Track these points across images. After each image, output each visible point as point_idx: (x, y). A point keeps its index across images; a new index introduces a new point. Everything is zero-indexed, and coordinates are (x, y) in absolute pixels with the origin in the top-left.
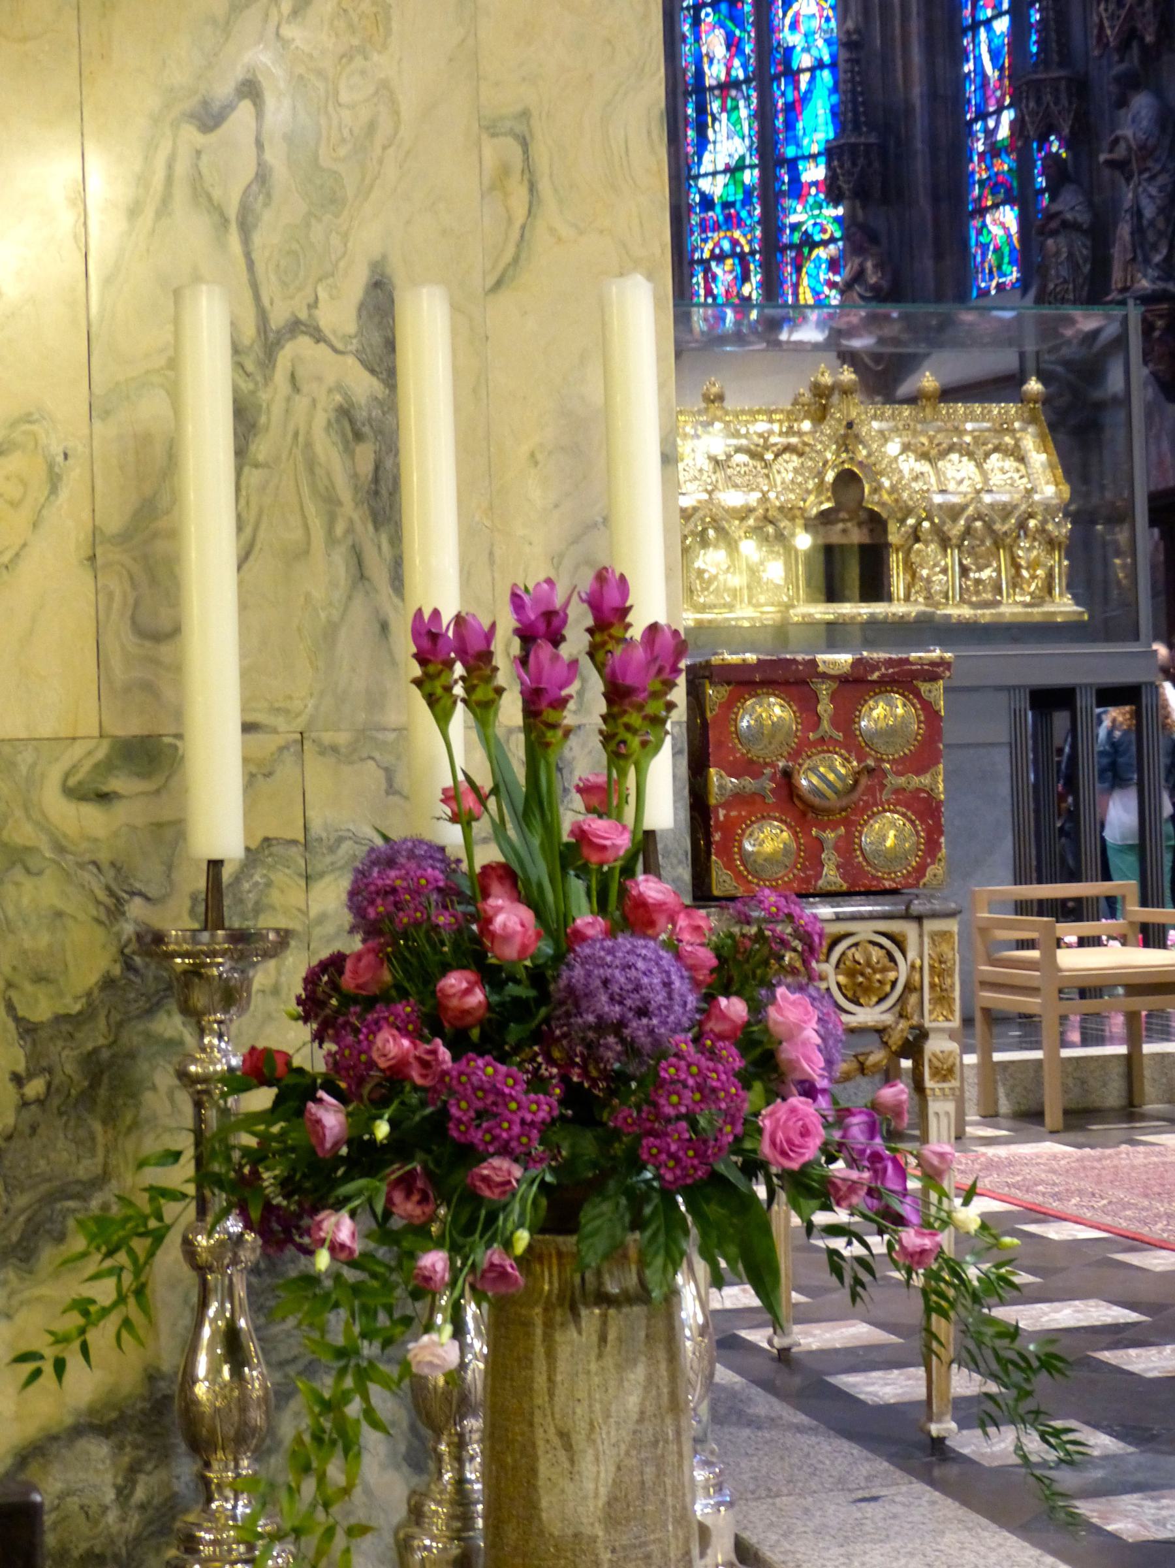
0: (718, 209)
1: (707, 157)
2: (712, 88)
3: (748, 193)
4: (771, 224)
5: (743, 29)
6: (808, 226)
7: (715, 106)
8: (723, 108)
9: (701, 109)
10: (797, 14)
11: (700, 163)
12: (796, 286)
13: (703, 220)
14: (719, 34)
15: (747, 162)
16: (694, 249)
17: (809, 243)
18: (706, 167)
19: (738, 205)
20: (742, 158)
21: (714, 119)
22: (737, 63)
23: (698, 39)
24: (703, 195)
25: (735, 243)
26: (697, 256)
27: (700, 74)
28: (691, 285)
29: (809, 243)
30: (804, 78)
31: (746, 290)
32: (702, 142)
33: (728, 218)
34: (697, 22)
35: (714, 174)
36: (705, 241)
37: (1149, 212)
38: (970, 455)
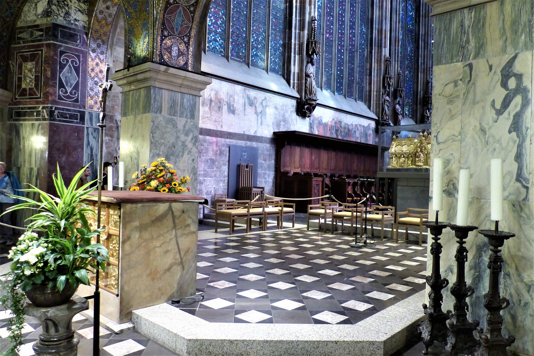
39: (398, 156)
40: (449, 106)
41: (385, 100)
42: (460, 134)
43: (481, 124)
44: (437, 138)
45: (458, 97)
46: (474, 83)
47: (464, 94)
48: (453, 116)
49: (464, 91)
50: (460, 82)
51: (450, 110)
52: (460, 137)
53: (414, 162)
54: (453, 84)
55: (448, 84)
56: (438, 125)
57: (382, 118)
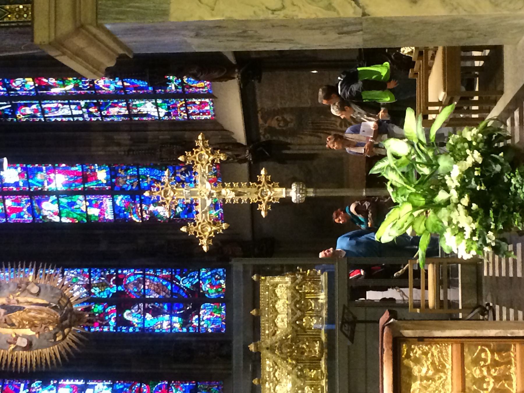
0: (170, 111)
1: (152, 114)
2: (129, 112)
3: (164, 102)
4: (176, 96)
5: (109, 102)
6: (176, 84)
7: (135, 111)
9: (136, 115)
10: (103, 86)
11: (154, 116)
12: (196, 88)
13: (174, 115)
14: (111, 110)
15: (154, 102)
16: (184, 118)
18: (156, 114)
19: (169, 105)
20: (152, 103)
21: (140, 111)
22: (120, 104)
23: (112, 116)
24: (165, 116)
26: (186, 118)
27: (124, 116)
28: (196, 120)
30: (125, 84)
31: (198, 103)
32: (147, 115)
33: (173, 108)
34: (106, 116)
35: (158, 112)
36: (181, 115)
38: (276, 301)
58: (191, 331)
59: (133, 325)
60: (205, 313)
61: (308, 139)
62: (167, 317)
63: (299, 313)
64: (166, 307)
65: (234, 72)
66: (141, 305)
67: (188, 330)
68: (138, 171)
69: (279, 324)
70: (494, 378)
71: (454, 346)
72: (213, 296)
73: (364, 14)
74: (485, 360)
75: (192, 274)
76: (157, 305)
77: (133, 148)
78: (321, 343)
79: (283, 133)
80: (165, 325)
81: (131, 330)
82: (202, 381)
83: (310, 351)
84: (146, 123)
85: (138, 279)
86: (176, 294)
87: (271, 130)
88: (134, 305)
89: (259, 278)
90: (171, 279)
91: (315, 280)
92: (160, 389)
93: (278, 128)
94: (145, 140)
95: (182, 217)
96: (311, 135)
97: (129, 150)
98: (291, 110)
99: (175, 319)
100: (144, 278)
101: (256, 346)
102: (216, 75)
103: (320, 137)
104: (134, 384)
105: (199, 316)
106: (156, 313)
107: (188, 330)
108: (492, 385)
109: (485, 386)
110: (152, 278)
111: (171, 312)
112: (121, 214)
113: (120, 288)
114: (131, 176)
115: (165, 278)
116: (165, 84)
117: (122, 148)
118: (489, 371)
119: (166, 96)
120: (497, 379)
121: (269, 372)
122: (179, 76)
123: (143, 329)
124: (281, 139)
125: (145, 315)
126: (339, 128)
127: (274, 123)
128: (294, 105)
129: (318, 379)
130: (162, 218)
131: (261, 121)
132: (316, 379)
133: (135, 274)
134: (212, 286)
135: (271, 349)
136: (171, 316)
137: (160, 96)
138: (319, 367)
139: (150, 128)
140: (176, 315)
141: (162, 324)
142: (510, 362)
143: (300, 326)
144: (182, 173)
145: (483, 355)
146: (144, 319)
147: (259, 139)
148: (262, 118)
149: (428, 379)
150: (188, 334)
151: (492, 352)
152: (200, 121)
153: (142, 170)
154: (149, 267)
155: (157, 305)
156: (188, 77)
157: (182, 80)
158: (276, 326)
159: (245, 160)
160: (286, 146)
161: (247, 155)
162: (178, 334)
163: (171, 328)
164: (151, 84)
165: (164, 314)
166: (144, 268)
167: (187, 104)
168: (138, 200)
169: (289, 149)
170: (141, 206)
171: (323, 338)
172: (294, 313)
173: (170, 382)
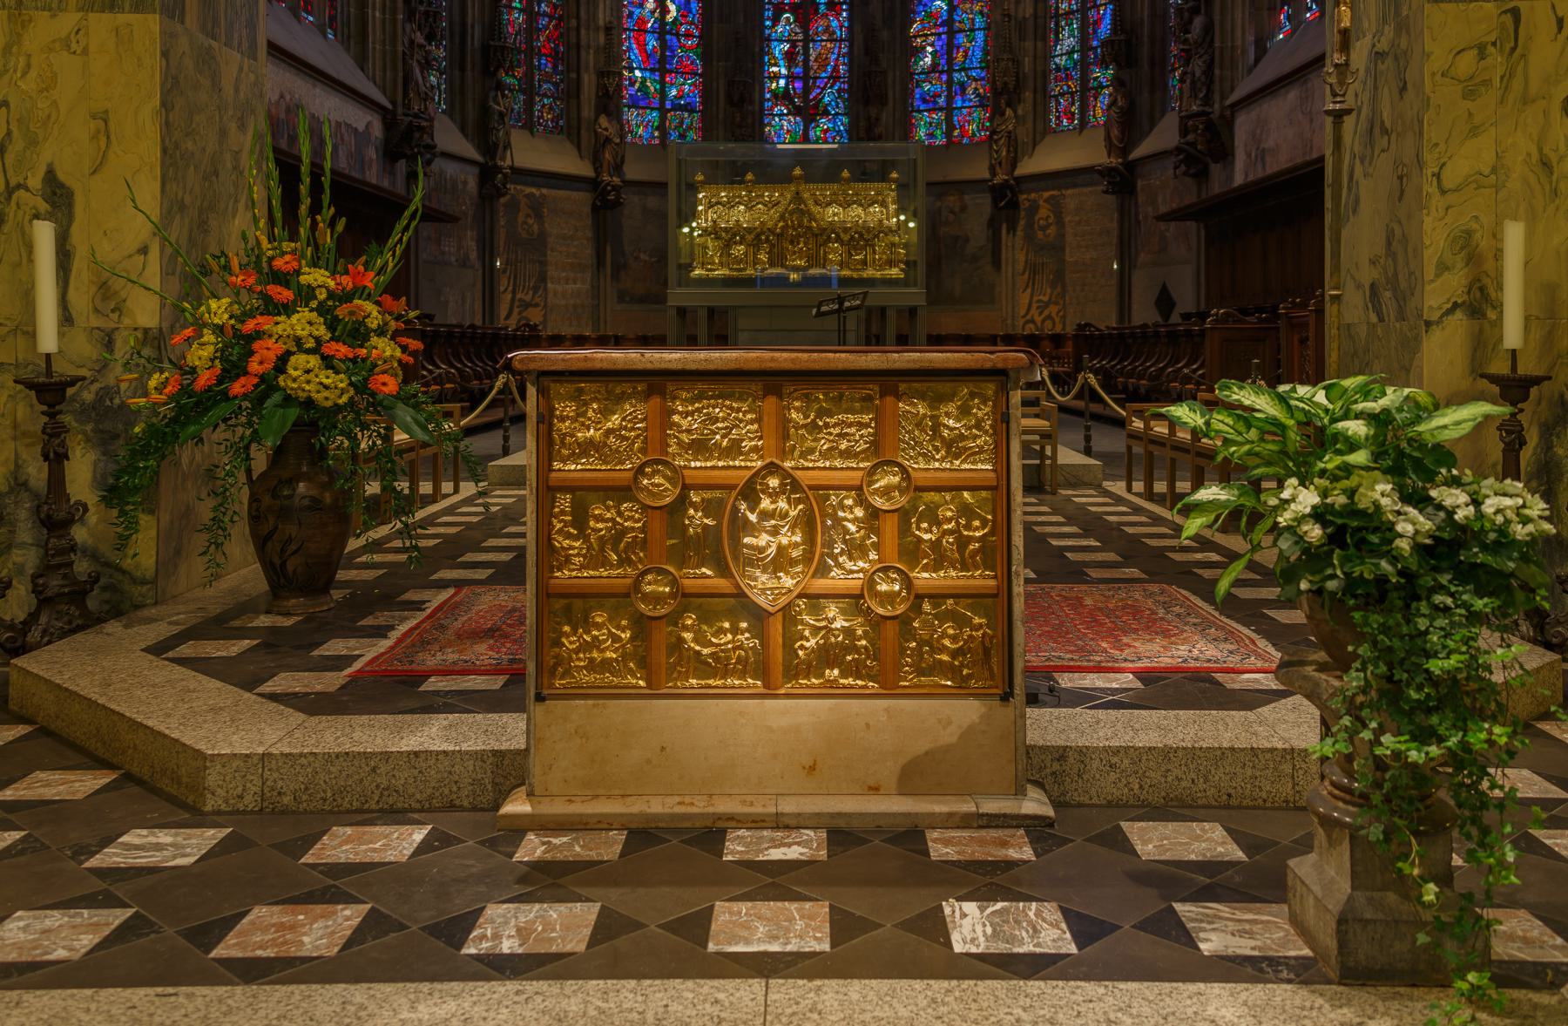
3: (1075, 64)
4: (1084, 79)
8: (1067, 24)
9: (1057, 24)
12: (1094, 107)
17: (1101, 86)
25: (1069, 87)
27: (1057, 8)
29: (1101, 86)
32: (1057, 40)
35: (1062, 55)
37: (1197, 75)
38: (861, 205)
39: (726, 237)
40: (1468, 104)
41: (412, 42)
42: (1494, 170)
43: (1540, 150)
44: (1438, 178)
45: (1487, 83)
46: (1523, 56)
47: (1502, 77)
48: (1477, 127)
49: (1500, 72)
50: (1491, 49)
51: (1470, 114)
52: (1493, 177)
53: (777, 259)
54: (1476, 51)
55: (1463, 50)
56: (1442, 147)
57: (407, 106)
58: (767, 105)
59: (774, 25)
60: (789, 122)
61: (1021, 257)
62: (784, 71)
63: (846, 238)
64: (798, 70)
65: (1118, 157)
66: (800, 37)
67: (768, 100)
68: (979, 29)
69: (830, 211)
70: (939, 540)
71: (993, 475)
72: (812, 134)
73: (1428, 324)
74: (968, 527)
75: (841, 105)
76: (800, 58)
77: (1013, 22)
78: (805, 269)
79: (1030, 225)
80: (775, 69)
81: (768, 23)
82: (702, 120)
83: (794, 253)
84: (1045, 38)
85: (834, 33)
86: (814, 82)
87: (1034, 208)
88: (801, 27)
89: (894, 181)
90: (835, 77)
91: (891, 263)
92: (692, 63)
93: (1037, 218)
94: (1022, 38)
95: (917, 91)
96: (1026, 262)
97: (1009, 16)
98: (1061, 236)
99: (782, 82)
100: (836, 40)
101: (800, 177)
102: (1115, 132)
103: (1023, 274)
104: (697, 27)
105: (787, 115)
106: (790, 57)
107: (768, 100)
108: (926, 537)
109: (925, 525)
110: (836, 51)
111: (790, 78)
112: (921, 8)
113: (822, 7)
114: (973, 20)
115: (835, 69)
116: (1103, 64)
117: (1012, 6)
118: (951, 532)
119: (1084, 66)
120: (936, 545)
121: (763, 196)
122: (1117, 82)
123: (769, 39)
124: (1022, 223)
125: (787, 41)
126: (1035, 299)
127: (1043, 212)
128: (1069, 238)
129: (755, 264)
130: (916, 63)
131: (1046, 195)
132: (756, 262)
133: (841, 27)
134: (825, 132)
135: (798, 197)
136: (787, 77)
137: (1084, 56)
138: (772, 265)
139: (1040, 44)
140: (787, 84)
141: (776, 65)
142: (964, 568)
143: (829, 239)
144: (976, 89)
145: (977, 523)
146: (781, 41)
147: (1022, 192)
148: (1052, 196)
149: (937, 427)
150: (763, 100)
151: (982, 539)
152: (1047, 111)
153: (980, 35)
154: (851, 47)
155: (800, 58)
156: (1110, 95)
157: (1107, 87)
158: (829, 204)
159: (994, 174)
160: (1012, 228)
161: (1000, 178)
162: (762, 85)
163: (769, 78)
164: (1104, 44)
165: (789, 68)
166: (851, 39)
167: (1072, 94)
168: (941, 29)
169: (1008, 233)
170: (932, 34)
171: (813, 271)
172: (846, 230)
173: (701, 75)
